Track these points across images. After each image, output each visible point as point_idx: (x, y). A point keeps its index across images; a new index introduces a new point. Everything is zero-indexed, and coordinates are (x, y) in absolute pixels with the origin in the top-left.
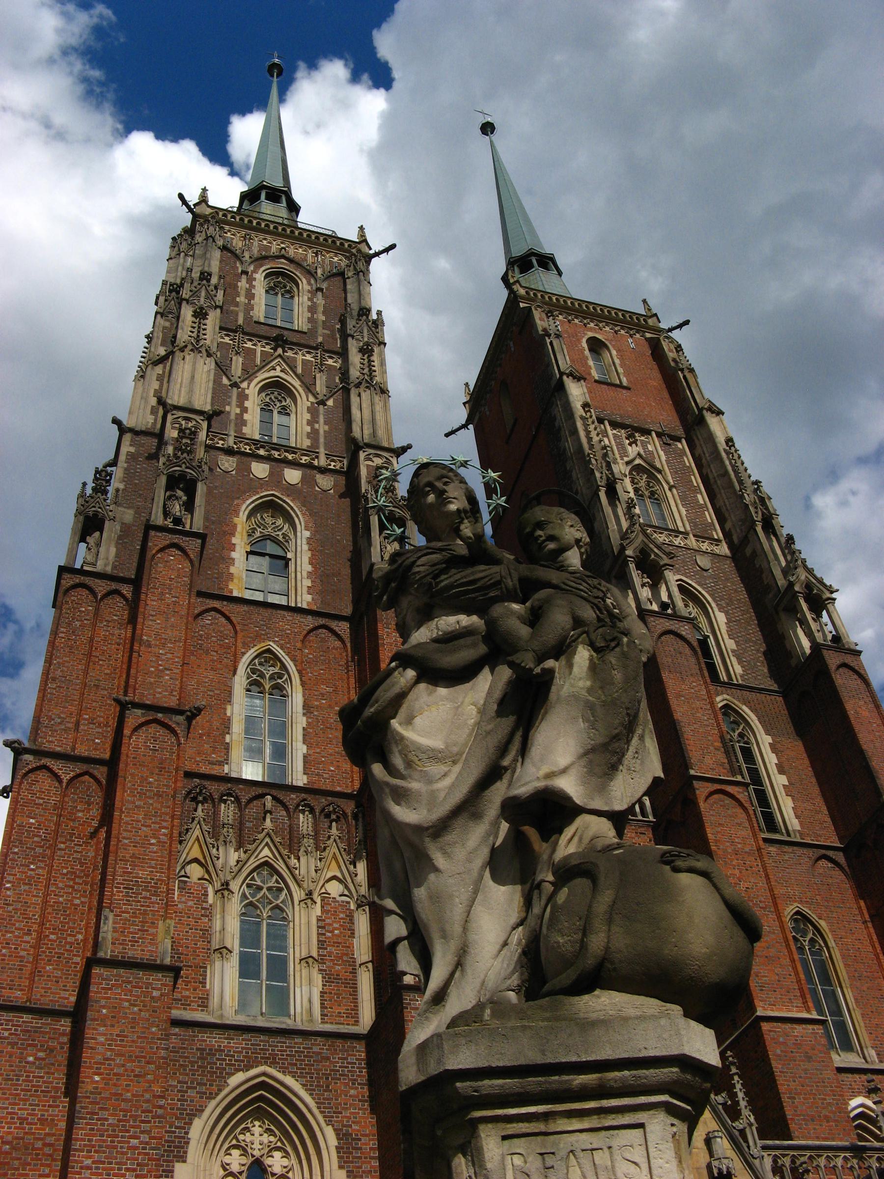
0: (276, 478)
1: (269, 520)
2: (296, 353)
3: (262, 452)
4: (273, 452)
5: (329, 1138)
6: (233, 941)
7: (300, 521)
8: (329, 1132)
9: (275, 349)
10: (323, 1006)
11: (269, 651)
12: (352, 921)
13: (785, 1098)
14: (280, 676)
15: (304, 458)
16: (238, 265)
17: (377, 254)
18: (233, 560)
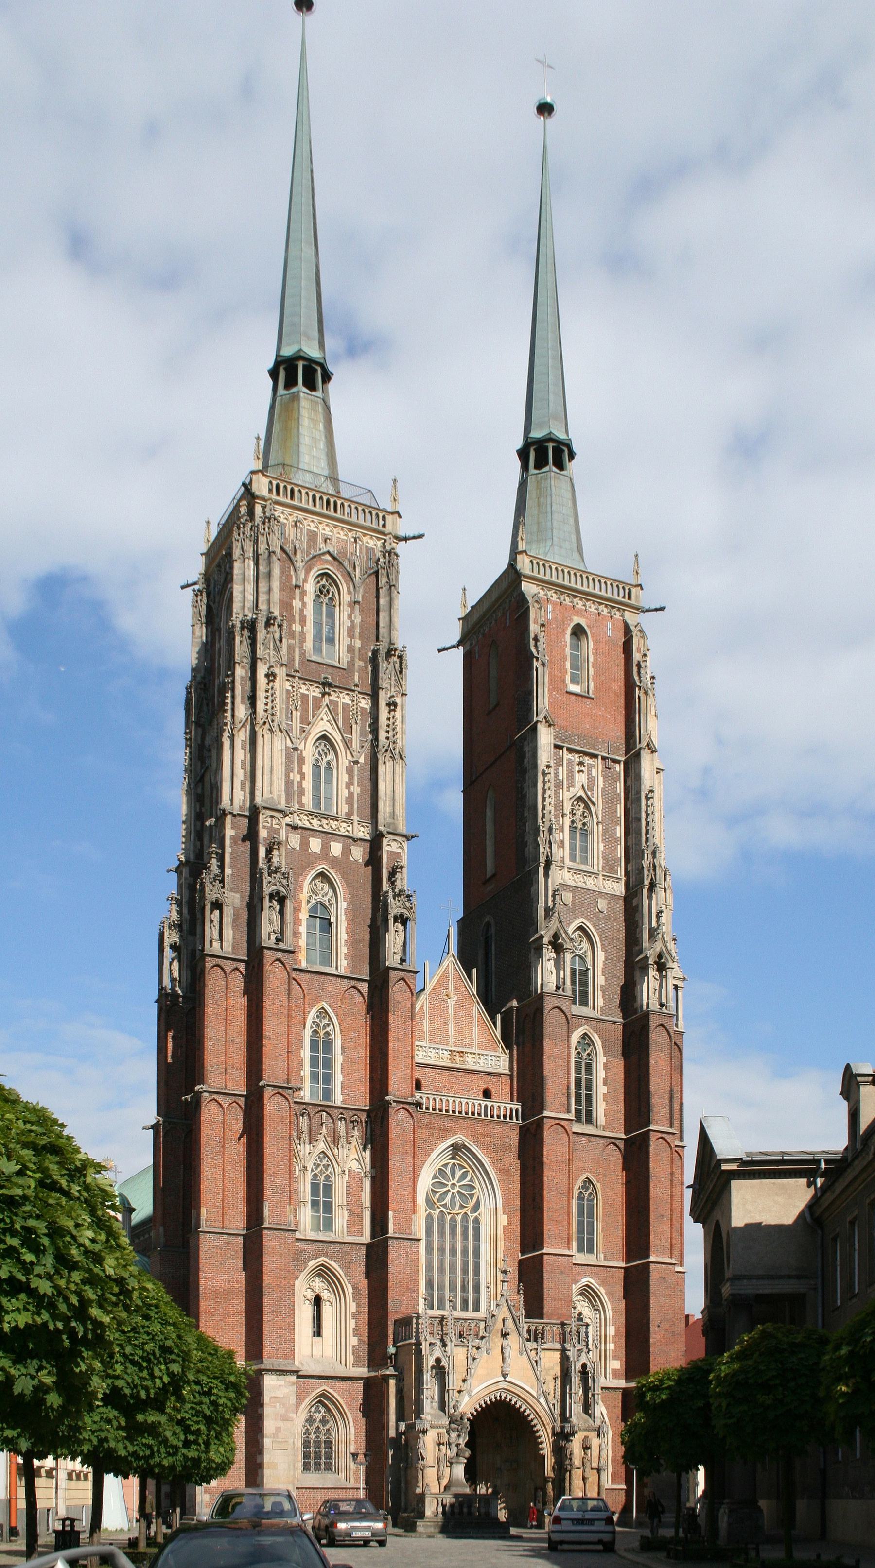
0: (326, 847)
1: (320, 885)
2: (338, 697)
3: (316, 824)
4: (324, 821)
5: (349, 1289)
6: (309, 1198)
7: (341, 891)
8: (350, 1286)
9: (324, 694)
10: (348, 1228)
11: (323, 1008)
12: (362, 1183)
13: (545, 1290)
14: (328, 1025)
15: (344, 825)
16: (292, 573)
17: (406, 539)
18: (300, 933)
